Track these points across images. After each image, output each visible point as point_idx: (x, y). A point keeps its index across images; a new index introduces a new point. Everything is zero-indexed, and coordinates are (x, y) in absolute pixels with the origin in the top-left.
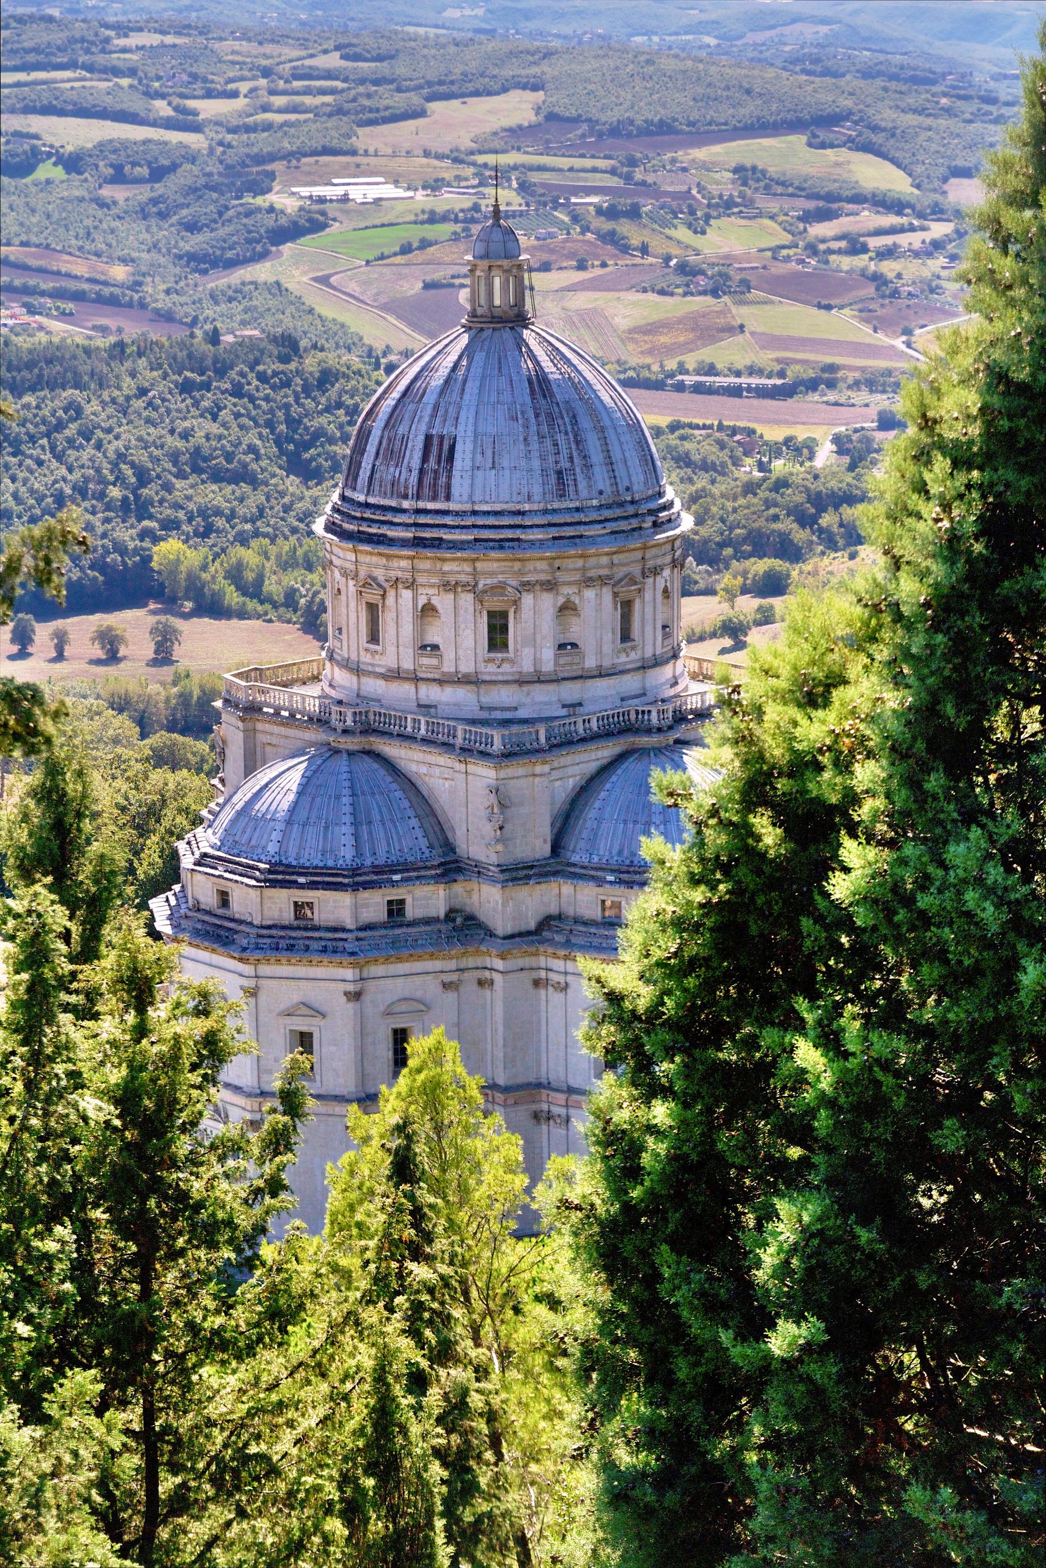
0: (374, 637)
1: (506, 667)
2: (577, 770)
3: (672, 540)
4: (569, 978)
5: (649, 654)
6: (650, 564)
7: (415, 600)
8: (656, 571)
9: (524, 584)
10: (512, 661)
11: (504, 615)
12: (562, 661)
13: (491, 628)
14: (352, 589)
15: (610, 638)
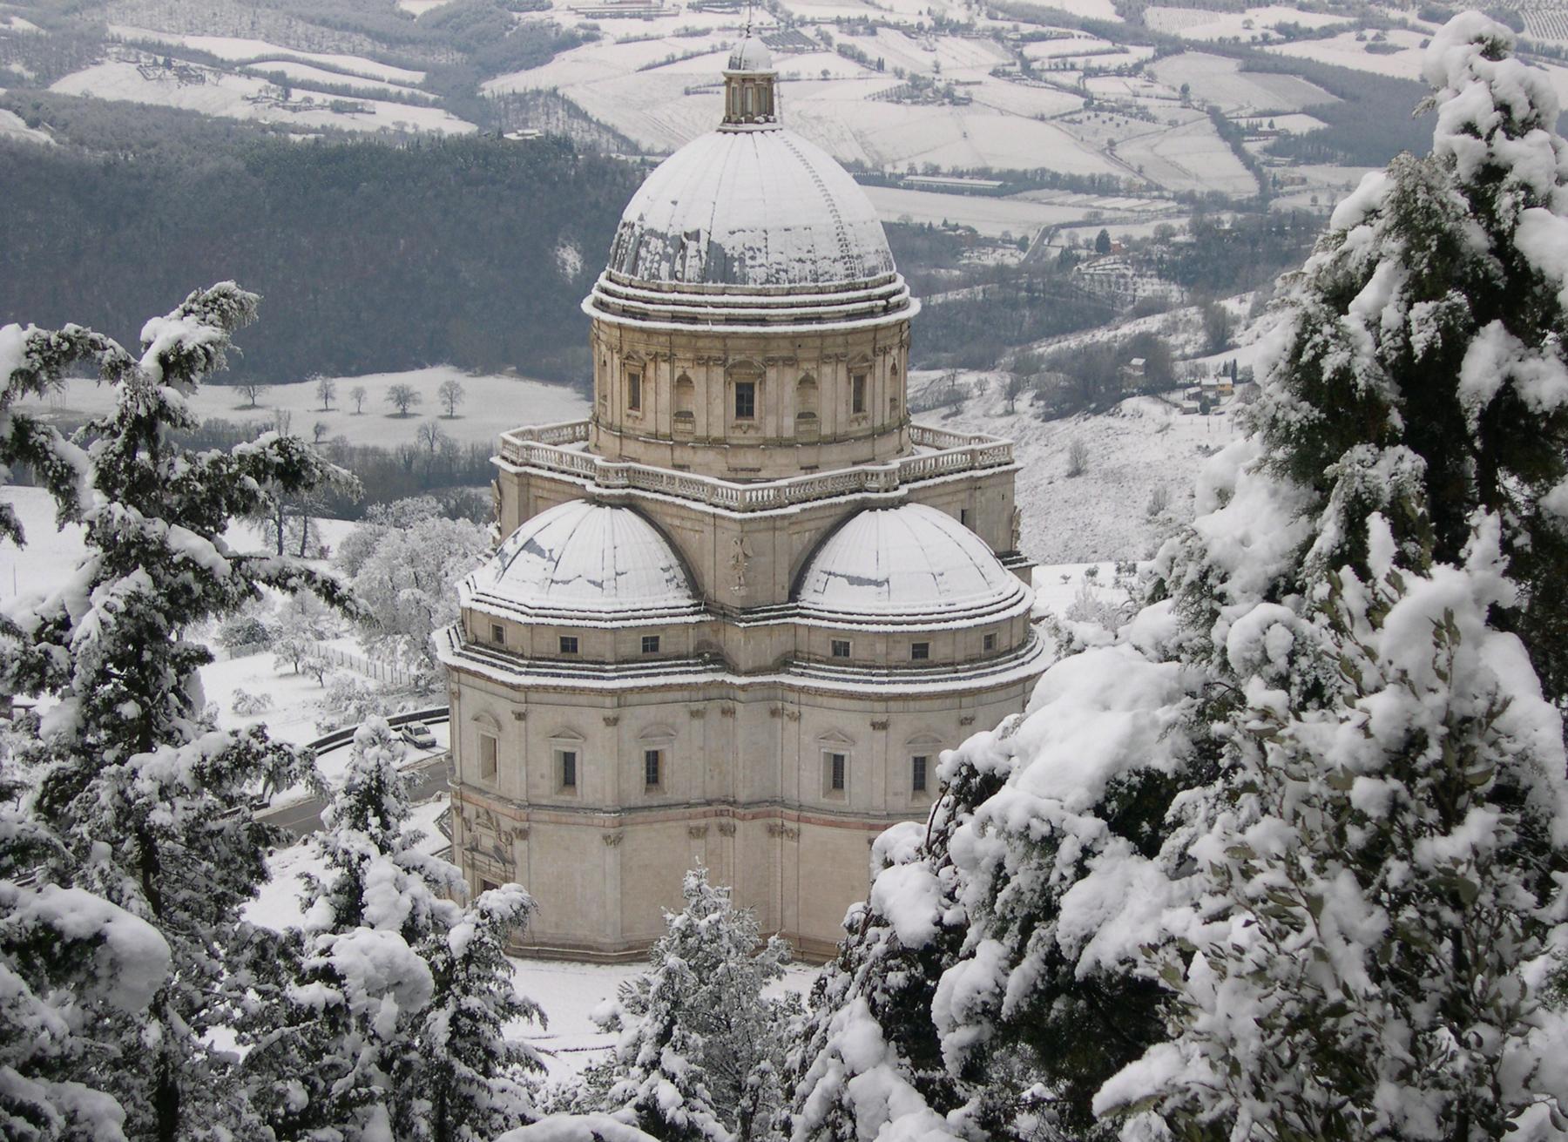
0: (635, 404)
1: (751, 433)
2: (812, 525)
3: (900, 324)
4: (804, 709)
5: (878, 423)
6: (880, 344)
7: (672, 372)
8: (885, 351)
9: (770, 359)
10: (757, 429)
11: (751, 387)
12: (802, 428)
13: (739, 398)
14: (617, 361)
15: (844, 411)
